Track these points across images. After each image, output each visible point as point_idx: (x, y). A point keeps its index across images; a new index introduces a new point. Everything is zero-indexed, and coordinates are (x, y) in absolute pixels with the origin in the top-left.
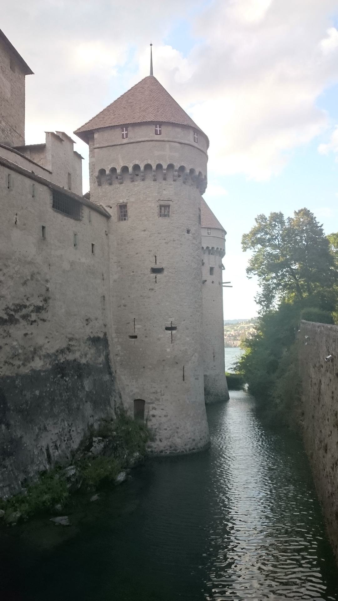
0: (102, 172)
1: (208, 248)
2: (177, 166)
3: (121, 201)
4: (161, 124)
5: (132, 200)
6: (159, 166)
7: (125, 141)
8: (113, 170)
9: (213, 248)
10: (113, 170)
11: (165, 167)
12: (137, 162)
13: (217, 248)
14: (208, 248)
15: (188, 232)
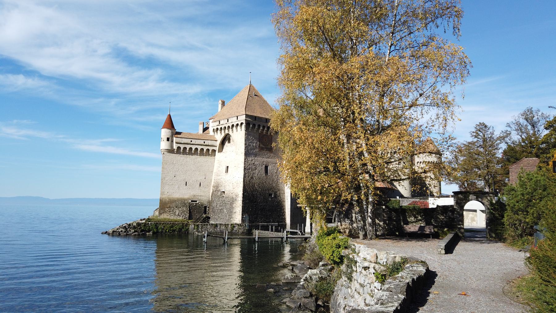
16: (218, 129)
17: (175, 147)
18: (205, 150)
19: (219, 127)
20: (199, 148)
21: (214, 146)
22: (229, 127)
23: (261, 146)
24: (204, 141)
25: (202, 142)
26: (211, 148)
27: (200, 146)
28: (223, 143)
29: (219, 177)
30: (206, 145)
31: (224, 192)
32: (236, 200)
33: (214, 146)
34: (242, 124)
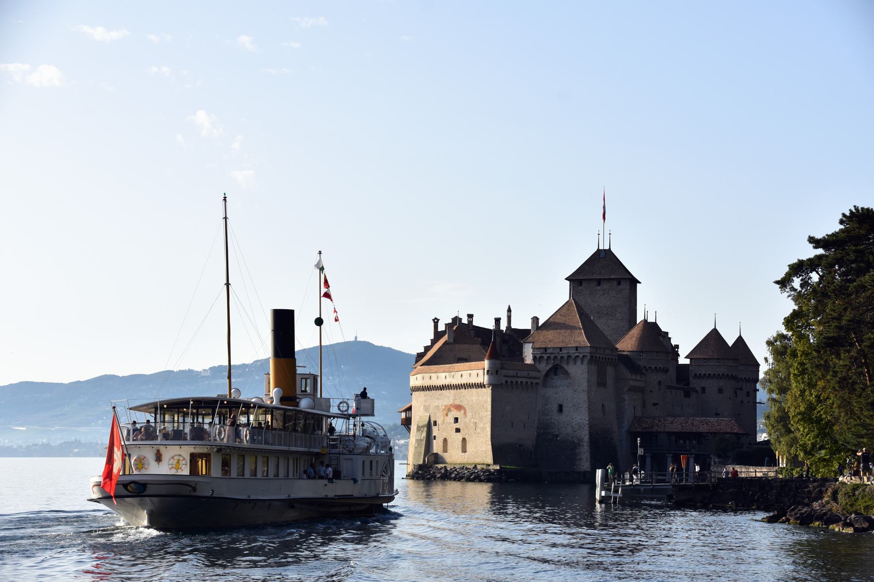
0: (696, 374)
1: (745, 378)
2: (726, 374)
3: (703, 386)
4: (719, 359)
5: (707, 386)
6: (719, 374)
7: (705, 364)
8: (700, 374)
9: (749, 378)
10: (700, 374)
11: (721, 375)
12: (710, 373)
13: (752, 378)
14: (745, 378)
15: (730, 399)
16: (541, 357)
17: (504, 380)
18: (529, 383)
19: (545, 356)
20: (524, 380)
21: (538, 378)
22: (562, 357)
23: (599, 381)
24: (529, 372)
25: (525, 374)
26: (534, 381)
27: (524, 379)
28: (547, 375)
29: (549, 417)
30: (530, 378)
31: (557, 436)
32: (579, 445)
33: (538, 378)
34: (584, 356)
